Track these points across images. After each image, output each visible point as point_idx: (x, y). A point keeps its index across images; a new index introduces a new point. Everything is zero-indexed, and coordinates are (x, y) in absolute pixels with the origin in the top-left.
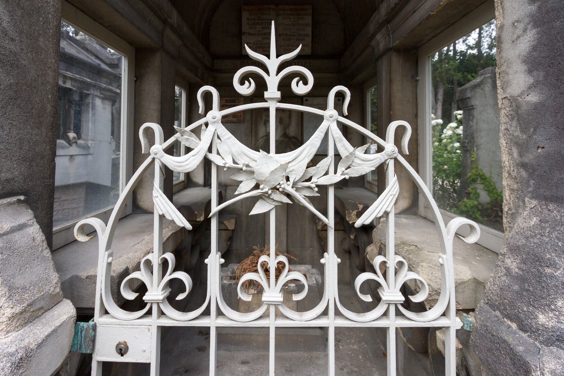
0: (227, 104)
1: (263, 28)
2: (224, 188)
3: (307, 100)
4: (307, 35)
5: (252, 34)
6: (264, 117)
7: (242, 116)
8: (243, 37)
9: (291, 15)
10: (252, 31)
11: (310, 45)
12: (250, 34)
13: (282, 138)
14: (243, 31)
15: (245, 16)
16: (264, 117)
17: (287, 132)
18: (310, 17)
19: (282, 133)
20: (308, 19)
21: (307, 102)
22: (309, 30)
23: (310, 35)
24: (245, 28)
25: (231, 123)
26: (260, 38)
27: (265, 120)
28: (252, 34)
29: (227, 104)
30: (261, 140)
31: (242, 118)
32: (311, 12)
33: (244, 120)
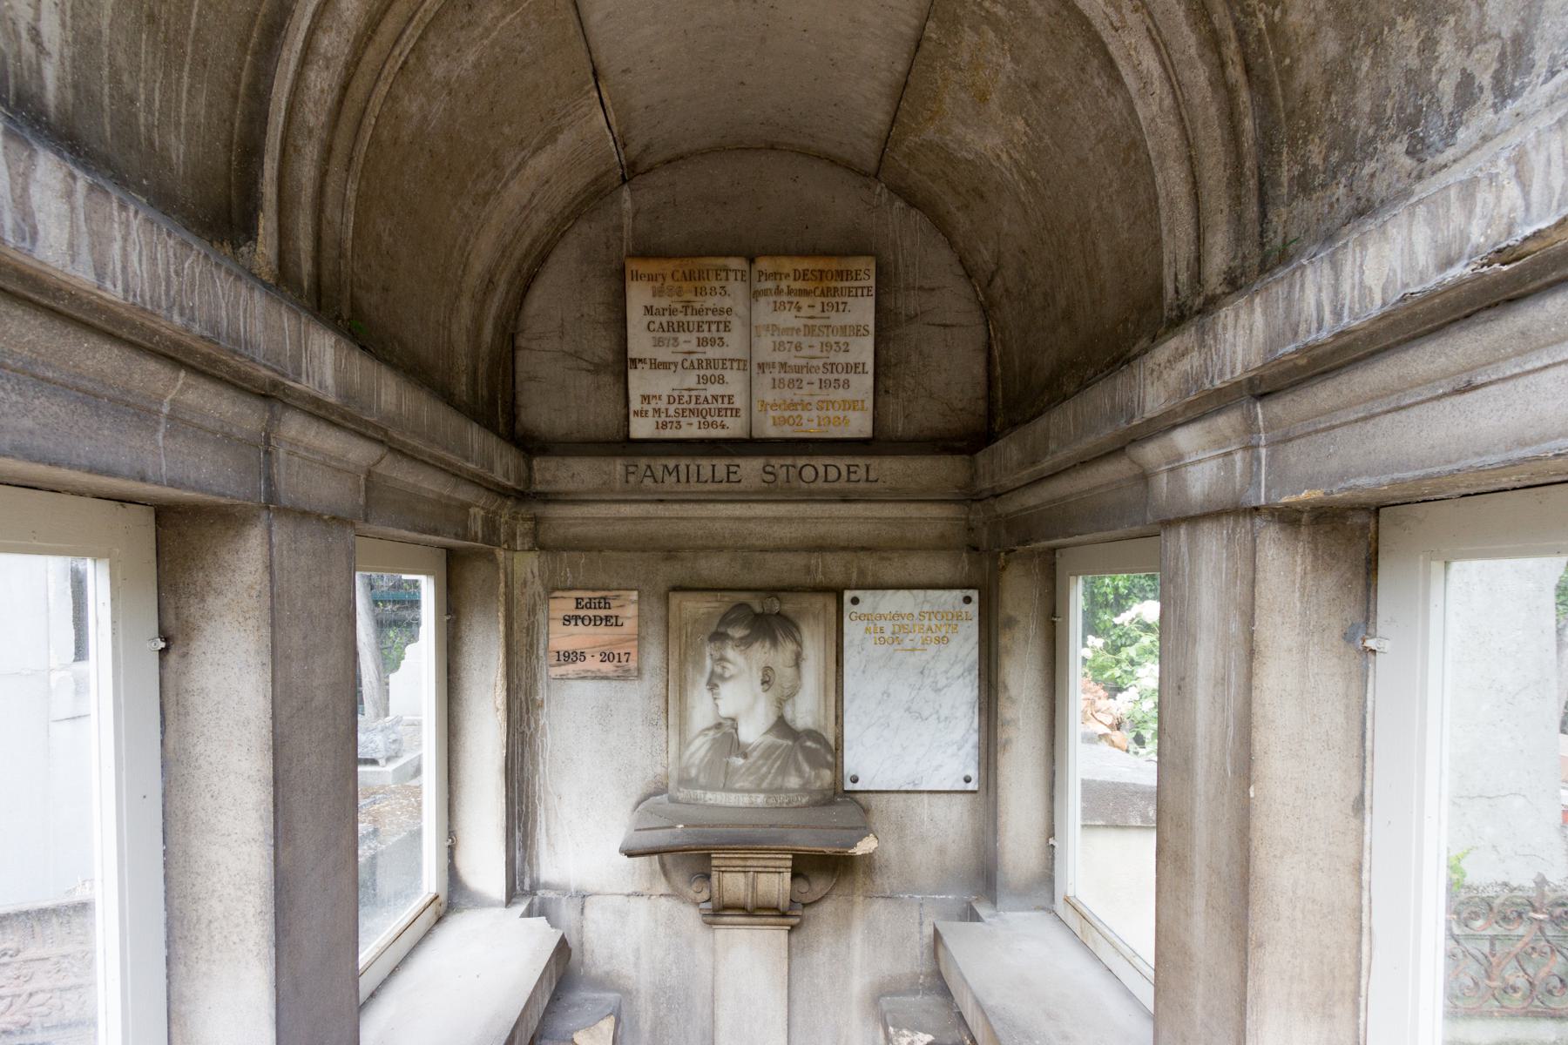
0: (582, 613)
1: (701, 342)
2: (578, 901)
3: (855, 601)
4: (855, 368)
5: (665, 366)
6: (708, 662)
7: (633, 657)
8: (633, 375)
9: (804, 293)
10: (663, 355)
11: (869, 403)
12: (656, 365)
13: (771, 739)
14: (632, 354)
15: (638, 296)
16: (708, 662)
17: (788, 716)
18: (870, 302)
19: (772, 719)
20: (863, 311)
21: (855, 608)
22: (863, 349)
23: (870, 367)
24: (640, 343)
25: (594, 678)
26: (691, 379)
27: (713, 673)
28: (665, 366)
29: (582, 613)
30: (698, 743)
31: (633, 664)
32: (872, 282)
33: (639, 670)
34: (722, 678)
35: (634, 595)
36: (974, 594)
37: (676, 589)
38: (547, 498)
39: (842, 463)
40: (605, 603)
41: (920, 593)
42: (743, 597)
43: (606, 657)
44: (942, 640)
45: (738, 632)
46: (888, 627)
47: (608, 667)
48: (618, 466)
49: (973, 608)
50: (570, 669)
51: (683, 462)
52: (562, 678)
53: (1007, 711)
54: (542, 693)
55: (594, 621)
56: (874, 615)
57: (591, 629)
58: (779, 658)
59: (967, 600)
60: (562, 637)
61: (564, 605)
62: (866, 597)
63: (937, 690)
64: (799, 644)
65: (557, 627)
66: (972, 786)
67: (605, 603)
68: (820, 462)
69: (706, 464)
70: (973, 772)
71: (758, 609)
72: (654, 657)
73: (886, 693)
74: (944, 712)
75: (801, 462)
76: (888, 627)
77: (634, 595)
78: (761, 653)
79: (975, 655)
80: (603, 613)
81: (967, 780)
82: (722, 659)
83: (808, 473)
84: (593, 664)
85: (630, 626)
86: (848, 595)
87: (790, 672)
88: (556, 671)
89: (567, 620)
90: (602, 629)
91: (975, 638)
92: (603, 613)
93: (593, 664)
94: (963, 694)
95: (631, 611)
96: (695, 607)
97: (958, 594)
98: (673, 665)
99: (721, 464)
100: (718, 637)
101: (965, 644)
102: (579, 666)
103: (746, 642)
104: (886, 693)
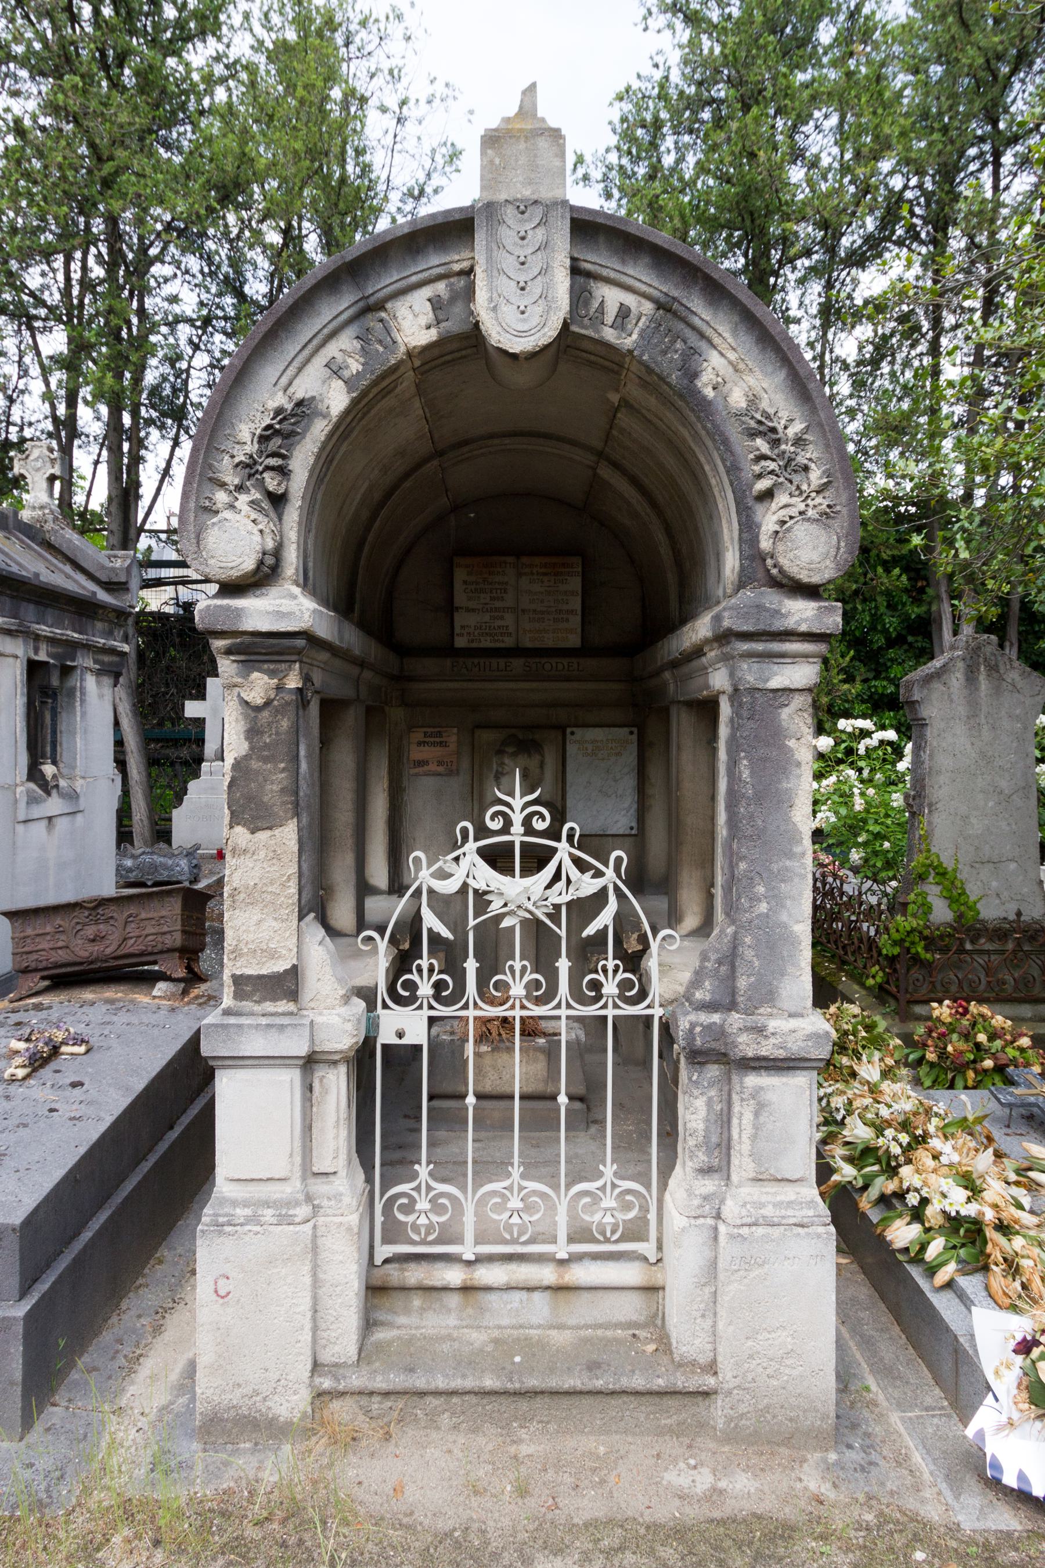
1: (492, 599)
3: (572, 733)
4: (572, 612)
5: (474, 610)
8: (456, 616)
9: (545, 574)
10: (472, 604)
11: (579, 630)
12: (468, 610)
14: (456, 605)
15: (460, 575)
18: (579, 579)
20: (575, 583)
22: (576, 603)
23: (579, 612)
24: (460, 598)
26: (487, 617)
28: (474, 610)
31: (454, 767)
32: (580, 569)
34: (503, 774)
35: (455, 730)
36: (635, 730)
37: (478, 727)
38: (410, 679)
39: (565, 661)
40: (440, 734)
41: (606, 729)
42: (513, 731)
43: (440, 763)
44: (619, 754)
45: (510, 750)
46: (590, 747)
47: (441, 769)
48: (448, 662)
49: (635, 737)
50: (420, 770)
51: (482, 661)
52: (417, 775)
53: (650, 791)
54: (405, 783)
55: (434, 744)
56: (582, 740)
57: (433, 748)
58: (533, 763)
59: (631, 733)
60: (417, 753)
61: (418, 735)
62: (579, 731)
63: (616, 781)
64: (543, 756)
65: (413, 747)
66: (634, 832)
67: (440, 734)
68: (553, 661)
69: (494, 662)
70: (634, 824)
71: (521, 737)
72: (465, 764)
73: (589, 783)
74: (619, 792)
75: (543, 660)
76: (590, 747)
77: (455, 730)
78: (523, 759)
79: (635, 762)
80: (438, 740)
81: (632, 828)
82: (503, 763)
83: (548, 666)
84: (433, 767)
85: (453, 746)
86: (569, 730)
87: (538, 771)
88: (413, 771)
89: (419, 744)
90: (438, 748)
91: (635, 754)
92: (438, 740)
93: (433, 767)
94: (629, 783)
95: (453, 739)
96: (487, 736)
97: (626, 730)
98: (476, 767)
99: (502, 662)
100: (500, 752)
101: (630, 757)
102: (426, 768)
103: (514, 755)
104: (589, 783)
